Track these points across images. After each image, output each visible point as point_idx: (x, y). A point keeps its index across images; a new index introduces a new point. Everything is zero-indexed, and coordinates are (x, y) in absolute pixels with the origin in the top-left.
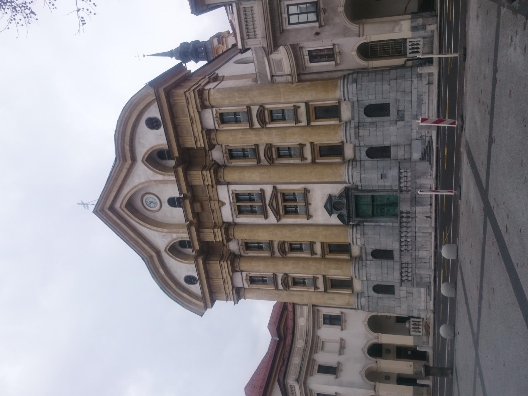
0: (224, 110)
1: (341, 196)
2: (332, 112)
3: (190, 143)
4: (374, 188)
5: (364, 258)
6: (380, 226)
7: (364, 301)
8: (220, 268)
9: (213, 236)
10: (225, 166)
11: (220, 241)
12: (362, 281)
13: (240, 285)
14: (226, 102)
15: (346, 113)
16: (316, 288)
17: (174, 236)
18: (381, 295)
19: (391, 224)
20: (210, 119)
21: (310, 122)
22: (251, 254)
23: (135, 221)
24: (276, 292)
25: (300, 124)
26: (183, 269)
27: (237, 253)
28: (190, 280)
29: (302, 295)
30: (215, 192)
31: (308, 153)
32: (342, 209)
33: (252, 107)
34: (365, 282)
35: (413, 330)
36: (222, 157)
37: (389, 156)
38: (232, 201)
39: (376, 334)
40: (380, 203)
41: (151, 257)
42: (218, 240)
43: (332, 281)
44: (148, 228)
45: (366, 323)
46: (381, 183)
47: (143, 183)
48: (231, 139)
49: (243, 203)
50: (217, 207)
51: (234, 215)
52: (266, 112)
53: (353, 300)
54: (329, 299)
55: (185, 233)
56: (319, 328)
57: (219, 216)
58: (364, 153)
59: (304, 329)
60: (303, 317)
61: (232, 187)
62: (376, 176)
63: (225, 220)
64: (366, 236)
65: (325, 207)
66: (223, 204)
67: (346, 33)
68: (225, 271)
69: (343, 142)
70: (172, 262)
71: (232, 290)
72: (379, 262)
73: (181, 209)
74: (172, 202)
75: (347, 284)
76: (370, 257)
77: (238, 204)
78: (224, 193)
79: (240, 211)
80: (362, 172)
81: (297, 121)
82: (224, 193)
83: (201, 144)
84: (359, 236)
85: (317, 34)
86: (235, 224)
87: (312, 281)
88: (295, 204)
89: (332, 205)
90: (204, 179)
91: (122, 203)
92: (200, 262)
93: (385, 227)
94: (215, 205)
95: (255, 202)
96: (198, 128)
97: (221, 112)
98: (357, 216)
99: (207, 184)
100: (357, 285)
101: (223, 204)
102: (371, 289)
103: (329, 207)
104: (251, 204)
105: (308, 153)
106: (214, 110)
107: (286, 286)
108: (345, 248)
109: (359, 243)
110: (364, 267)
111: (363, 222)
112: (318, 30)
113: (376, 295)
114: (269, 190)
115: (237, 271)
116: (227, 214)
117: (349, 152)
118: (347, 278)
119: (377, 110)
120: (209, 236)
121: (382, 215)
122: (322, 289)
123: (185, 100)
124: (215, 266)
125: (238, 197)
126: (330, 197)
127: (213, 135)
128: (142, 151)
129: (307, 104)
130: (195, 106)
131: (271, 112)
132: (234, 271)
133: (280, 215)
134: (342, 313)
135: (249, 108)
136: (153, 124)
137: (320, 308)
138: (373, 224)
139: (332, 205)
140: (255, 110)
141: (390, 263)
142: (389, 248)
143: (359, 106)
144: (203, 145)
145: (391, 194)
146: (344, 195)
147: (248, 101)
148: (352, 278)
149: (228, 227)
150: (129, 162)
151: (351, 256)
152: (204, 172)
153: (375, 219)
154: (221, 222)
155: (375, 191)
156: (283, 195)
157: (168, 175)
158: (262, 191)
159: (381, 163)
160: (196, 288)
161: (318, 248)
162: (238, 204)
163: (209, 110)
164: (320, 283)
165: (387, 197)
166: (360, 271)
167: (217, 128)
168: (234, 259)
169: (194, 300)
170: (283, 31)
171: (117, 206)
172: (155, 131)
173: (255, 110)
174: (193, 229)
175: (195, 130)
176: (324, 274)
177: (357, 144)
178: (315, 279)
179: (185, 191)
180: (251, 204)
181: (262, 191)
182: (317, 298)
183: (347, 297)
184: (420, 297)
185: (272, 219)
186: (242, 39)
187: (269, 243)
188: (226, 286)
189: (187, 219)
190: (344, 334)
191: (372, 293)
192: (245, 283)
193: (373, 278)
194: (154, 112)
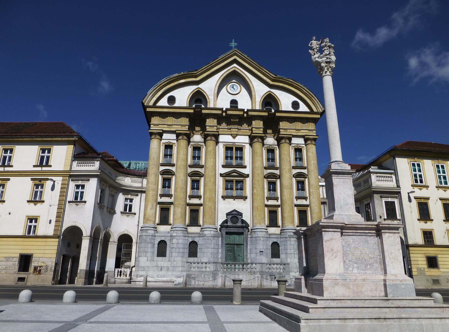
1: (243, 222)
3: (283, 125)
4: (248, 246)
5: (190, 235)
6: (218, 249)
7: (151, 232)
10: (263, 145)
11: (206, 129)
12: (169, 232)
13: (165, 136)
16: (162, 196)
18: (156, 246)
19: (220, 257)
21: (297, 207)
23: (224, 73)
24: (158, 164)
25: (295, 200)
26: (183, 96)
27: (192, 140)
28: (172, 100)
29: (155, 184)
30: (244, 134)
32: (232, 222)
34: (169, 235)
35: (120, 271)
36: (268, 144)
37: (272, 257)
38: (236, 144)
39: (116, 240)
40: (235, 249)
41: (196, 77)
42: (207, 127)
43: (168, 209)
44: (218, 80)
45: (126, 233)
46: (254, 251)
47: (253, 87)
48: (286, 153)
49: (234, 152)
50: (232, 133)
51: (225, 144)
52: (303, 179)
54: (152, 204)
55: (214, 106)
56: (123, 194)
57: (225, 133)
58: (275, 240)
62: (262, 248)
63: (220, 136)
64: (212, 238)
65: (235, 210)
66: (234, 137)
68: (179, 128)
69: (279, 227)
70: (189, 90)
71: (162, 130)
73: (229, 107)
74: (234, 103)
75: (164, 221)
76: (191, 240)
77: (234, 148)
79: (228, 148)
80: (265, 239)
81: (297, 198)
83: (282, 132)
84: (212, 232)
85: (381, 217)
86: (217, 142)
87: (167, 193)
88: (234, 189)
89: (235, 216)
90: (256, 128)
91: (238, 69)
92: (192, 111)
93: (218, 253)
94: (234, 131)
95: (236, 160)
97: (303, 150)
98: (227, 233)
99: (253, 129)
101: (234, 137)
102: (163, 239)
103: (235, 212)
104: (234, 157)
106: (304, 146)
107: (164, 173)
108: (194, 222)
110: (184, 235)
111: (222, 237)
112: (383, 218)
113: (156, 243)
115: (177, 137)
116: (225, 139)
117: (272, 230)
118: (171, 220)
120: (211, 123)
121: (227, 251)
122: (160, 200)
123: (310, 128)
124: (185, 121)
125: (240, 149)
126: (241, 214)
127: (288, 141)
129: (307, 206)
130: (307, 134)
133: (226, 177)
134: (135, 214)
135: (305, 168)
136: (295, 105)
138: (220, 243)
139: (235, 216)
140: (305, 171)
141: (187, 255)
142: (199, 254)
144: (281, 133)
145: (245, 258)
146: (244, 225)
148: (171, 225)
149: (216, 137)
150: (271, 83)
151: (188, 226)
152: (262, 130)
153: (224, 245)
154: (220, 133)
155: (247, 247)
156: (242, 181)
157: (260, 105)
158: (245, 167)
159: (269, 252)
160: (164, 102)
162: (234, 148)
163: (303, 142)
164: (166, 200)
165: (240, 255)
166: (181, 232)
167: (292, 145)
169: (155, 99)
170: (381, 197)
171: (235, 65)
172: (291, 105)
173: (305, 171)
174: (220, 112)
175: (292, 131)
176: (176, 203)
177: (282, 236)
178: (170, 196)
179: (250, 113)
180: (234, 157)
181: (245, 167)
183: (153, 220)
184: (158, 277)
186: (376, 173)
187: (199, 165)
188: (166, 126)
189: (227, 109)
191: (158, 240)
192: (167, 141)
193: (175, 241)
194: (303, 108)
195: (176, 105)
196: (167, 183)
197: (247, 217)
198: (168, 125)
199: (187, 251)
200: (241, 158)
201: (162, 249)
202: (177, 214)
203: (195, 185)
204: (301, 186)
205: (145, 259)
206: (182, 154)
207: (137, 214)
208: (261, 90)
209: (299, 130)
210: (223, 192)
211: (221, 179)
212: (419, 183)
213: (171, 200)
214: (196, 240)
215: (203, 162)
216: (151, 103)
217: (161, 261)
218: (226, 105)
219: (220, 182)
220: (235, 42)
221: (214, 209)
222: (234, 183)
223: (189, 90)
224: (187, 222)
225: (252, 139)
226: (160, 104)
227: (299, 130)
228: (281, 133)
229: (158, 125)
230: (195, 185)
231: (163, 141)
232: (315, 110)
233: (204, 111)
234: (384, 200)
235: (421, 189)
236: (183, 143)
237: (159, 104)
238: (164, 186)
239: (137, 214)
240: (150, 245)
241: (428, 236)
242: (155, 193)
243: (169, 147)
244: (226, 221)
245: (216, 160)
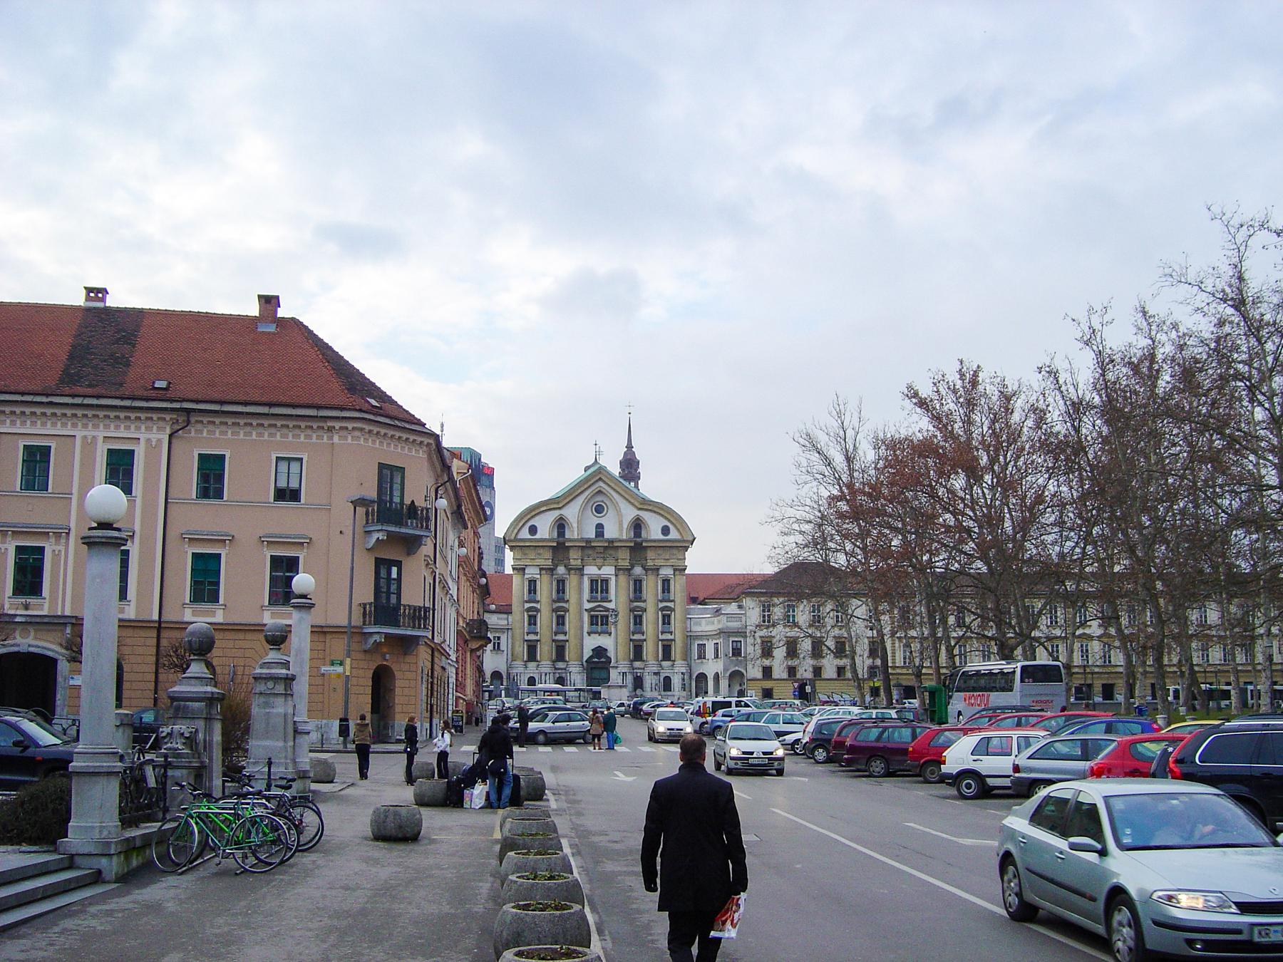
0: (672, 582)
2: (667, 655)
3: (650, 554)
8: (546, 559)
9: (575, 558)
17: (575, 525)
20: (666, 572)
22: (555, 583)
28: (533, 530)
31: (636, 637)
43: (535, 647)
49: (600, 586)
61: (613, 578)
67: (725, 670)
75: (532, 656)
78: (608, 571)
79: (593, 582)
83: (650, 563)
89: (600, 652)
94: (599, 561)
96: (659, 562)
100: (532, 665)
105: (636, 637)
107: (529, 610)
114: (611, 606)
117: (637, 664)
124: (548, 554)
125: (606, 582)
128: (646, 516)
131: (669, 616)
136: (665, 530)
140: (671, 605)
147: (678, 600)
149: (580, 571)
160: (525, 534)
161: (561, 637)
168: (551, 571)
171: (601, 484)
173: (671, 605)
178: (536, 633)
182: (518, 632)
185: (588, 606)
194: (674, 534)
195: (537, 536)
196: (532, 621)
197: (611, 654)
202: (545, 650)
203: (561, 621)
204: (667, 620)
206: (545, 590)
208: (629, 513)
215: (567, 597)
218: (591, 533)
225: (618, 569)
226: (521, 536)
234: (732, 639)
236: (546, 578)
238: (530, 624)
241: (767, 672)
244: (591, 657)
245: (579, 597)
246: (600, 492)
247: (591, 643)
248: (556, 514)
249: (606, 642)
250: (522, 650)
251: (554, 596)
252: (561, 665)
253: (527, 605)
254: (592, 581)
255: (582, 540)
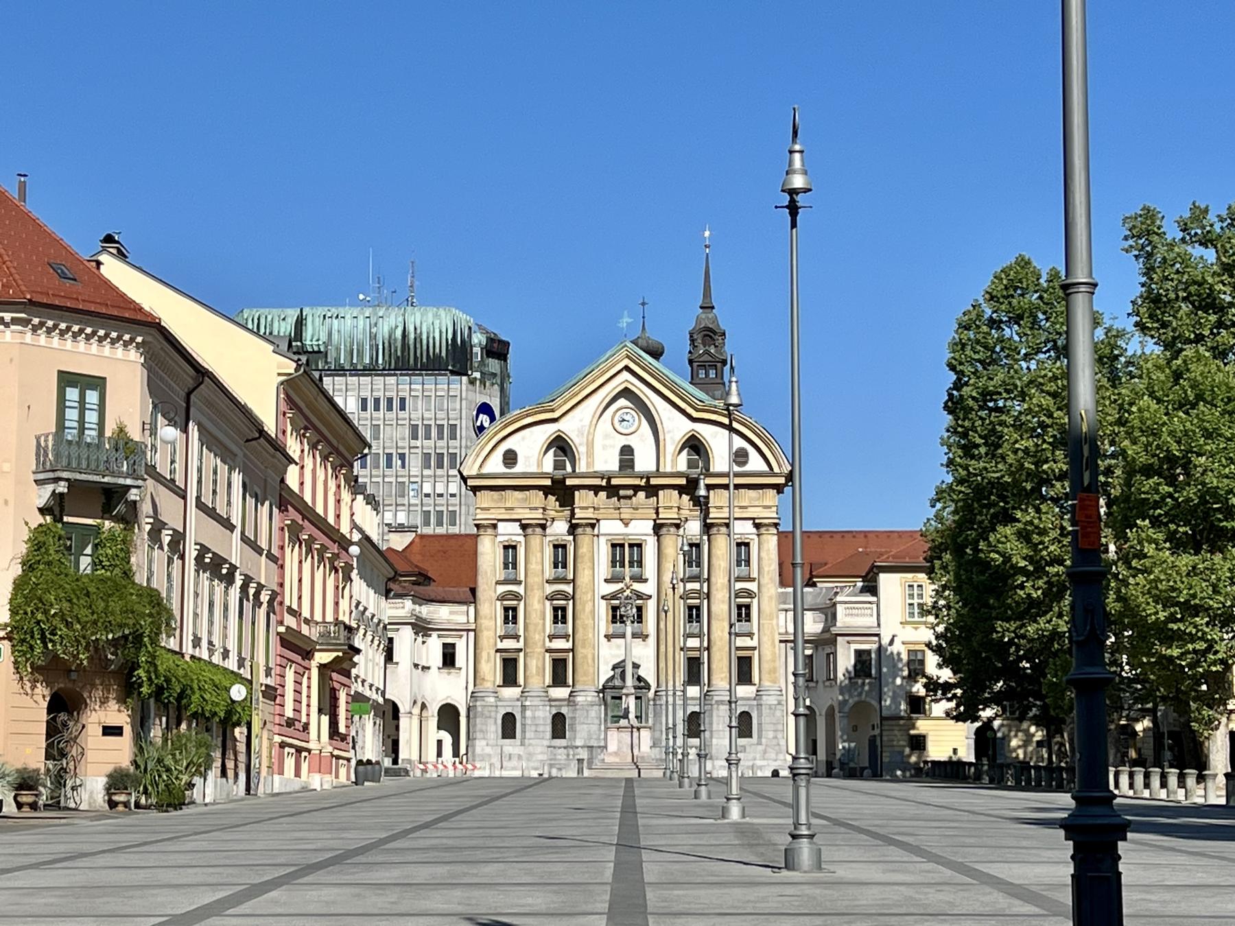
14: (763, 554)
15: (743, 691)
16: (502, 638)
18: (500, 722)
20: (743, 529)
28: (510, 458)
33: (755, 584)
41: (553, 411)
50: (623, 516)
53: (488, 685)
55: (588, 467)
59: (435, 616)
60: (451, 613)
66: (626, 525)
72: (549, 721)
74: (627, 451)
76: (554, 712)
82: (642, 528)
84: (589, 699)
90: (665, 508)
92: (548, 482)
100: (511, 692)
101: (626, 525)
109: (579, 699)
111: (606, 705)
114: (649, 588)
119: (744, 725)
122: (500, 646)
127: (724, 529)
129: (754, 649)
132: (524, 527)
137: (464, 638)
141: (549, 734)
143: (750, 706)
150: (695, 414)
158: (646, 581)
164: (509, 644)
178: (517, 637)
181: (646, 581)
186: (846, 603)
190: (434, 670)
192: (506, 538)
194: (755, 463)
198: (506, 509)
199: (549, 728)
200: (640, 564)
201: (509, 726)
204: (744, 612)
205: (484, 743)
207: (464, 671)
208: (676, 427)
209: (745, 507)
210: (607, 628)
211: (603, 603)
212: (916, 619)
213: (520, 645)
214: (564, 711)
216: (474, 472)
217: (510, 746)
219: (603, 609)
220: (630, 317)
221: (596, 659)
222: (625, 613)
223: (544, 433)
224: (548, 679)
227: (745, 507)
228: (711, 516)
229: (488, 509)
230: (559, 615)
231: (500, 538)
232: (776, 470)
233: (569, 482)
235: (916, 628)
237: (485, 470)
239: (464, 671)
240: (492, 721)
242: (492, 633)
243: (510, 548)
246: (626, 393)
247: (610, 653)
248: (549, 430)
249: (644, 654)
250: (492, 670)
251: (549, 572)
252: (561, 693)
253: (502, 589)
254: (614, 546)
255: (594, 475)
